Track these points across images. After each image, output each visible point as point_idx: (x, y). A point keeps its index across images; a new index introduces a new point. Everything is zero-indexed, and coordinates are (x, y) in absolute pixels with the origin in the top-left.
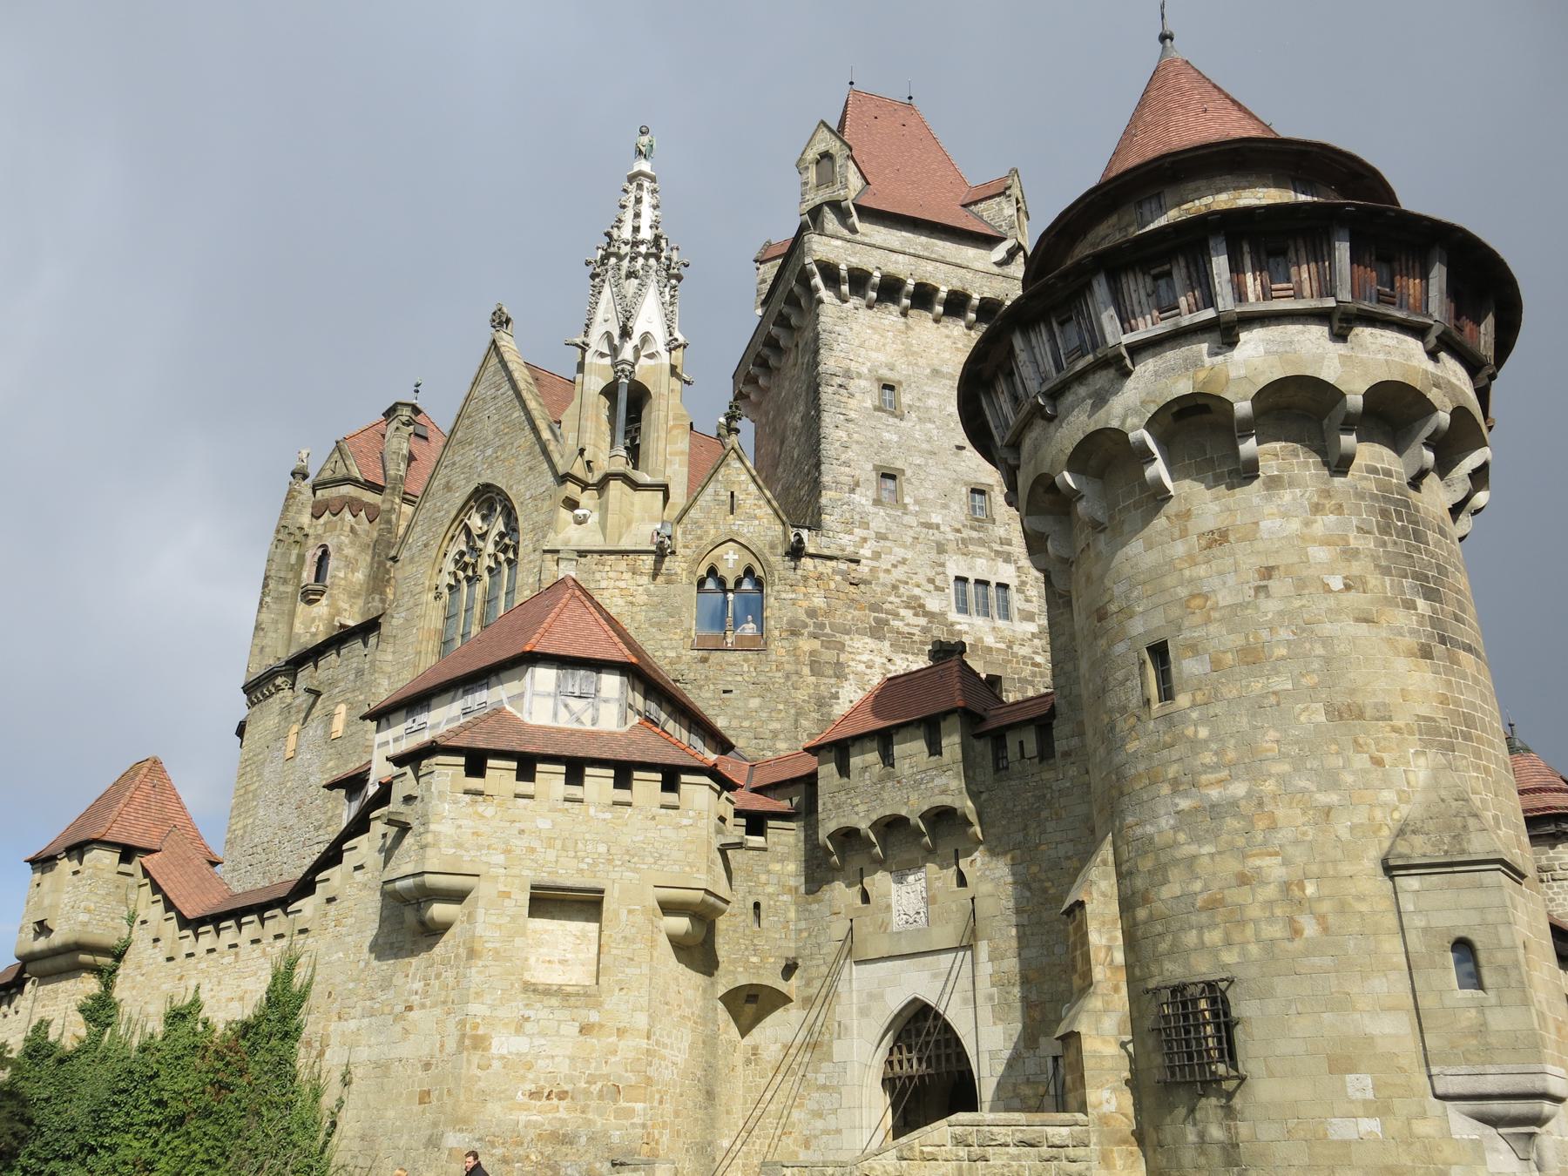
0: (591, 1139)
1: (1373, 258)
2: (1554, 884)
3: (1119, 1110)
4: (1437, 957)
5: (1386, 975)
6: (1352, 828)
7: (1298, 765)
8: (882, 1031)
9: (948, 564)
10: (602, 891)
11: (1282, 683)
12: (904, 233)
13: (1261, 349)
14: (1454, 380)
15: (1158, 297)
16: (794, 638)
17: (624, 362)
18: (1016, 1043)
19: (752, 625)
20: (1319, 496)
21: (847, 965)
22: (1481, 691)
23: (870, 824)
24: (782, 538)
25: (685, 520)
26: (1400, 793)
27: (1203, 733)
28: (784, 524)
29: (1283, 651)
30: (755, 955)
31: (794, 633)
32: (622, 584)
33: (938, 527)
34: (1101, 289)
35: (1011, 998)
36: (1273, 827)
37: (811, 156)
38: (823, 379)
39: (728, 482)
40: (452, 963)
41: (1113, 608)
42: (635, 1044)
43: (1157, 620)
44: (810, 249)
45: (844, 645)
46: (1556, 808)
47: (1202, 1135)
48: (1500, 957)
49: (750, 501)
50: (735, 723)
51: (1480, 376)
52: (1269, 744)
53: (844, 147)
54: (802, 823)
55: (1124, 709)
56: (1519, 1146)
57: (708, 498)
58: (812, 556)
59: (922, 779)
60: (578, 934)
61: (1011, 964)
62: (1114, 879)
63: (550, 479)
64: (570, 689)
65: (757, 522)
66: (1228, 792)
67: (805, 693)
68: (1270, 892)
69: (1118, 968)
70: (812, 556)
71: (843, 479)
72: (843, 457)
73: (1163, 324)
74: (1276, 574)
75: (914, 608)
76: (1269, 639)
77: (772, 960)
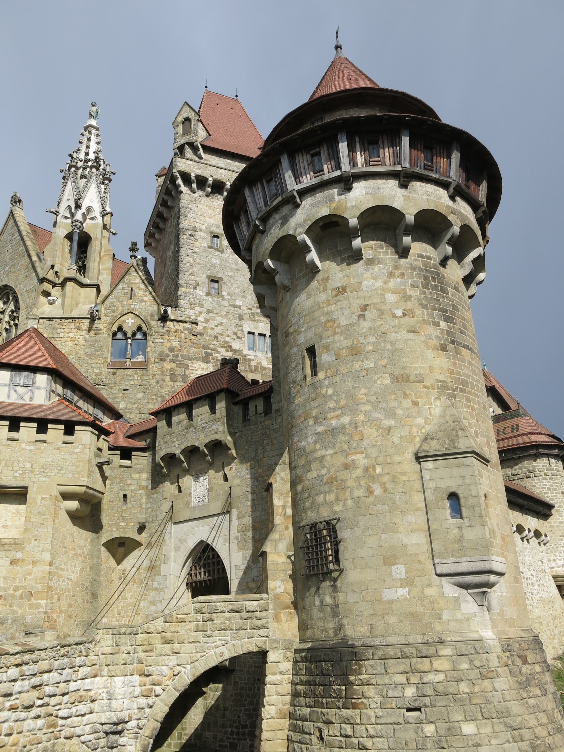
0: (14, 621)
1: (422, 147)
2: (535, 478)
3: (285, 591)
4: (440, 502)
5: (414, 513)
6: (401, 438)
7: (375, 405)
8: (185, 558)
9: (244, 325)
10: (27, 488)
11: (369, 364)
12: (227, 160)
13: (364, 192)
14: (463, 212)
15: (314, 166)
16: (162, 362)
17: (77, 221)
18: (249, 561)
19: (141, 356)
20: (393, 269)
21: (170, 525)
22: (472, 369)
23: (180, 451)
24: (157, 311)
25: (106, 302)
26: (426, 419)
27: (330, 391)
28: (158, 304)
29: (370, 348)
30: (123, 522)
31: (162, 359)
32: (72, 335)
33: (240, 307)
34: (285, 162)
35: (247, 537)
36: (362, 439)
37: (180, 119)
38: (181, 231)
39: (130, 283)
41: (292, 330)
42: (42, 569)
43: (311, 334)
44: (176, 165)
45: (188, 366)
46: (536, 442)
47: (322, 602)
48: (471, 501)
49: (141, 293)
50: (129, 406)
51: (479, 212)
52: (359, 396)
53: (196, 115)
54: (151, 453)
55: (295, 382)
56: (478, 599)
57: (119, 291)
58: (173, 321)
59: (206, 426)
60: (14, 511)
61: (248, 520)
62: (288, 471)
63: (36, 281)
64: (18, 382)
65: (144, 303)
66: (341, 421)
67: (166, 390)
68: (359, 472)
69: (288, 517)
70: (173, 321)
71: (191, 282)
72: (191, 271)
73: (315, 179)
74: (369, 308)
75: (226, 347)
76: (364, 342)
77: (132, 524)
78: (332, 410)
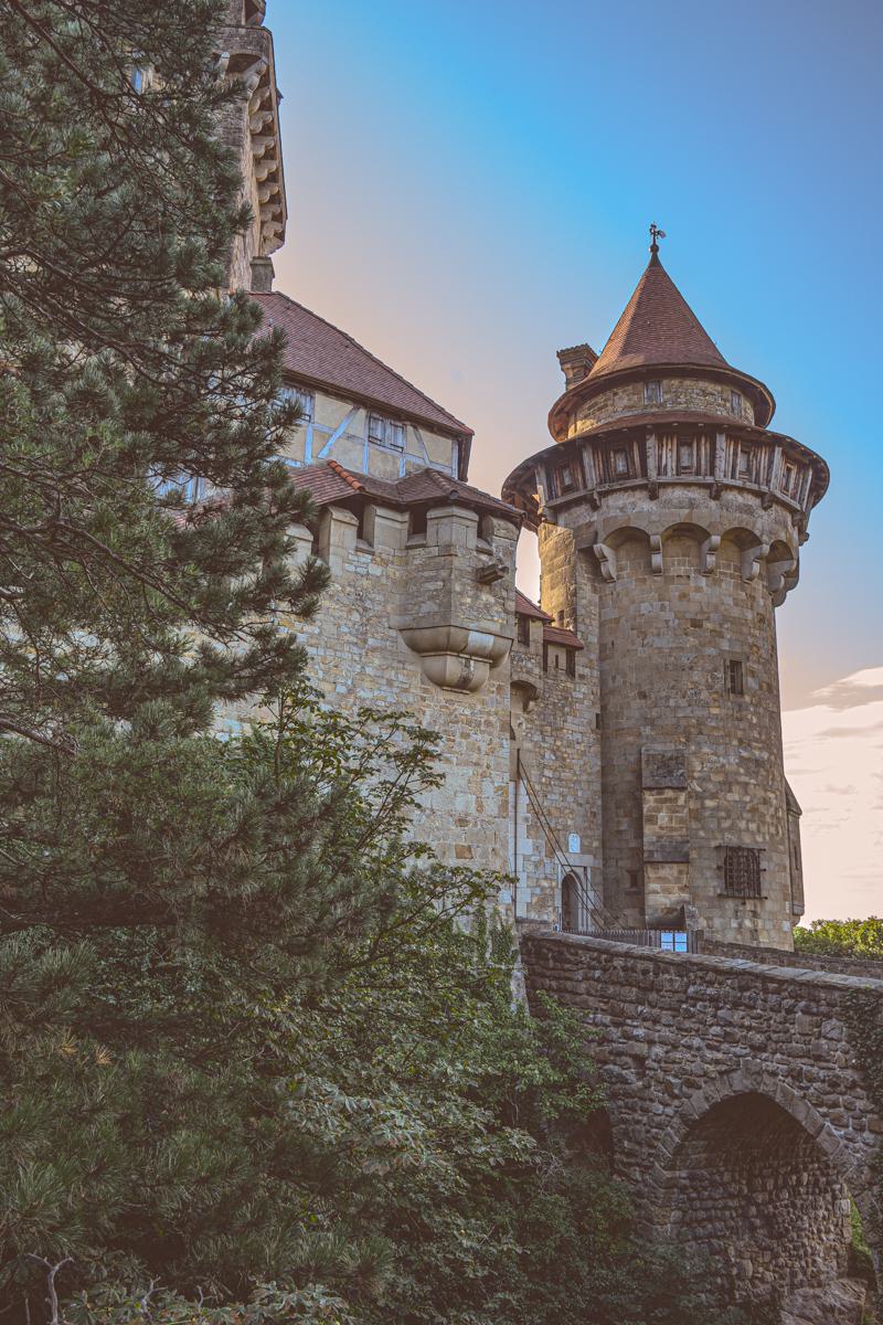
40: (482, 728)
47: (740, 926)
78: (756, 740)
